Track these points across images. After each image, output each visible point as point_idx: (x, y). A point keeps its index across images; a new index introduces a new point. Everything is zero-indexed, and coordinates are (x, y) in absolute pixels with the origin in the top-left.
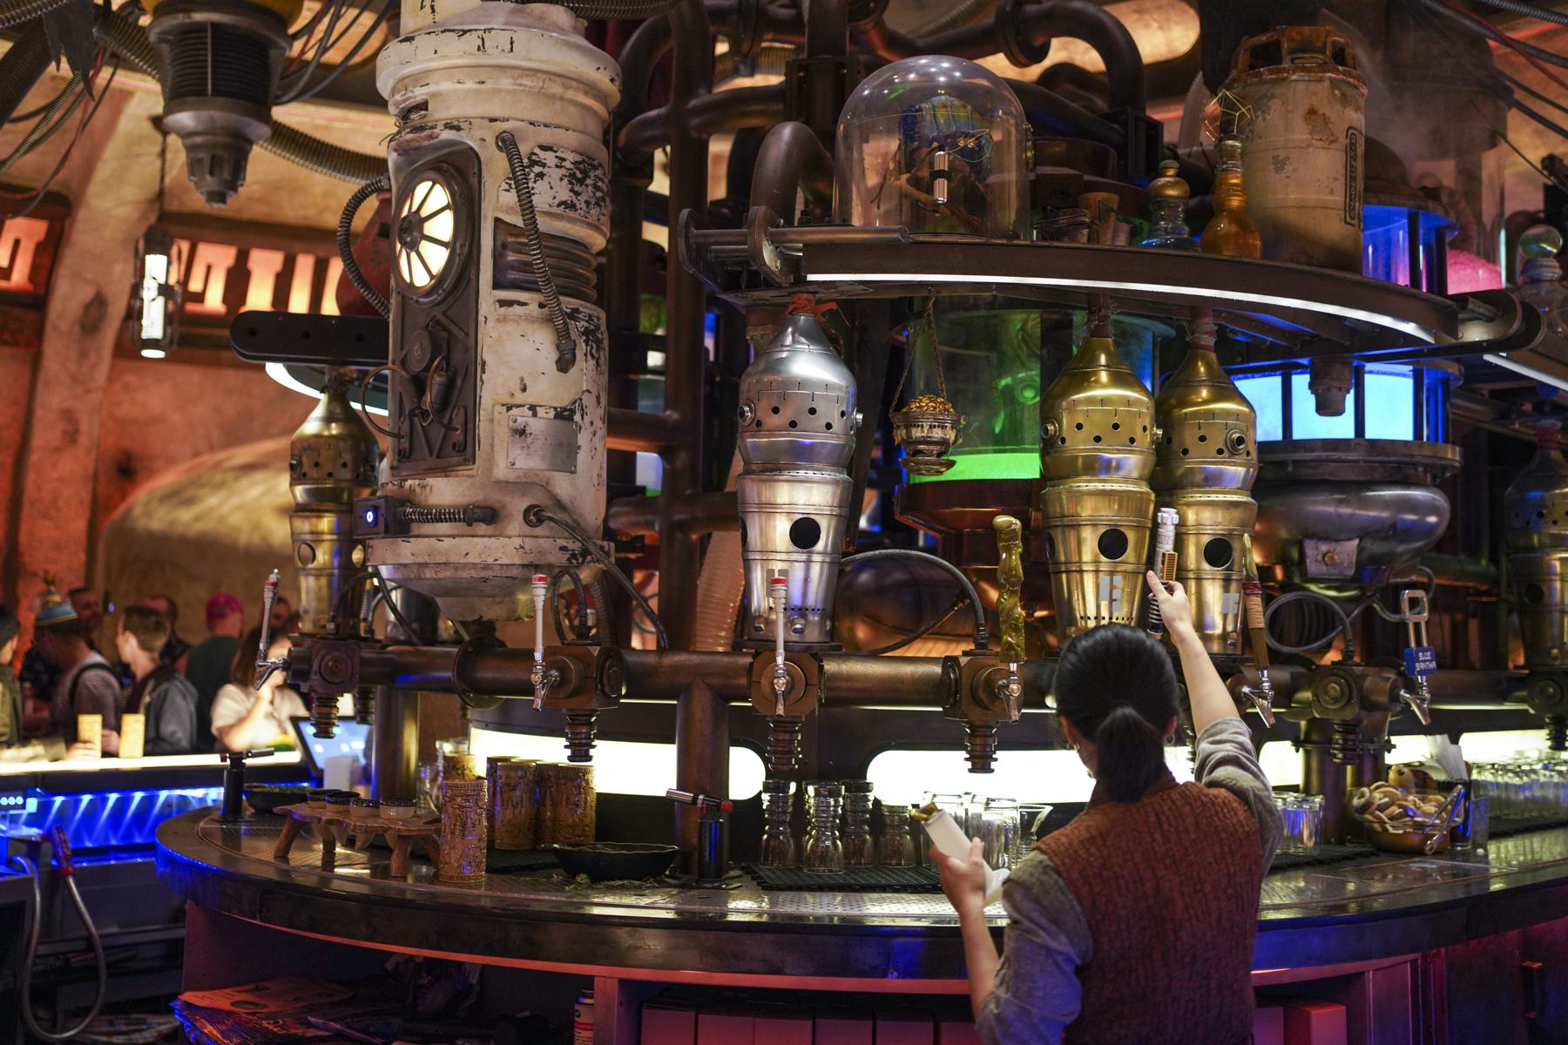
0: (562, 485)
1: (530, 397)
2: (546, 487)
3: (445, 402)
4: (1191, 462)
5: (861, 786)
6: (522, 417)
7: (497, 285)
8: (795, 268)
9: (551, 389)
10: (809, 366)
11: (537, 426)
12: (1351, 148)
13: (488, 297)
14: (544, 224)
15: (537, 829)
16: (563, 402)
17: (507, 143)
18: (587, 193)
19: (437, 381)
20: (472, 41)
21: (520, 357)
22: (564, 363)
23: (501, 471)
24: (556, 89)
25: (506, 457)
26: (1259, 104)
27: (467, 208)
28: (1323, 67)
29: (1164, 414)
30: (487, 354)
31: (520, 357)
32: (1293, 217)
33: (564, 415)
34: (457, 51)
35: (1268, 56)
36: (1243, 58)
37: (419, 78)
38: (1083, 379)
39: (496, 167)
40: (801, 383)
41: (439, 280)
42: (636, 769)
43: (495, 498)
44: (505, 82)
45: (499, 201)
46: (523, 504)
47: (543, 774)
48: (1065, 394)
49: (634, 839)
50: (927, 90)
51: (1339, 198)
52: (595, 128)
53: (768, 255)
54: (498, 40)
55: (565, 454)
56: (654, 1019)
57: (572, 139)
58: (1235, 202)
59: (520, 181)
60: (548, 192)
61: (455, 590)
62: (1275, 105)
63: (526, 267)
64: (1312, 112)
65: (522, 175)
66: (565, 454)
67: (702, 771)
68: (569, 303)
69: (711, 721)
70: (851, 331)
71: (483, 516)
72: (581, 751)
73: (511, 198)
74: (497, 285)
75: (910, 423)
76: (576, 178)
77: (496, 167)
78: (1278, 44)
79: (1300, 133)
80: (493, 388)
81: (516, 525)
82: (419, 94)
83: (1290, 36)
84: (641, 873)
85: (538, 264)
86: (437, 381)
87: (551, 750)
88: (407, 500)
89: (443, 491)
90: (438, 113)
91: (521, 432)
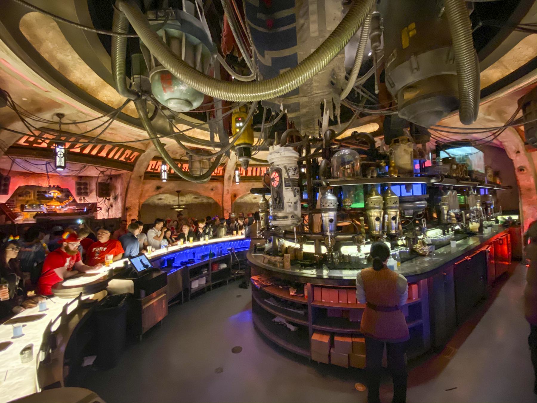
0: (296, 212)
1: (291, 201)
2: (294, 213)
3: (279, 202)
4: (389, 205)
5: (340, 252)
6: (290, 204)
7: (285, 186)
8: (328, 185)
9: (293, 200)
10: (331, 197)
11: (292, 205)
12: (411, 155)
13: (284, 188)
14: (291, 177)
15: (295, 256)
16: (295, 201)
17: (285, 167)
18: (296, 172)
19: (278, 199)
20: (279, 154)
21: (289, 196)
22: (295, 196)
23: (288, 211)
24: (291, 159)
25: (288, 209)
26: (396, 149)
27: (280, 176)
28: (406, 143)
29: (384, 199)
30: (285, 196)
31: (289, 196)
32: (403, 166)
33: (295, 203)
34: (278, 155)
35: (397, 141)
36: (393, 142)
37: (272, 159)
38: (372, 195)
39: (284, 171)
40: (330, 200)
41: (277, 186)
42: (309, 248)
43: (287, 215)
44: (284, 159)
45: (285, 175)
46: (291, 215)
47: (296, 250)
48: (368, 197)
49: (309, 261)
50: (345, 154)
51: (410, 162)
52: (296, 163)
53: (324, 183)
54: (283, 153)
55: (296, 208)
56: (315, 288)
57: (294, 165)
58: (393, 165)
59: (287, 172)
60: (291, 173)
61: (283, 227)
62: (399, 149)
63: (289, 183)
64: (405, 150)
65: (287, 171)
66: (296, 208)
67: (318, 249)
68: (295, 187)
69: (319, 242)
70: (337, 192)
71: (285, 217)
72: (301, 246)
73: (286, 175)
74: (285, 186)
75: (345, 203)
76: (294, 171)
77: (284, 171)
78: (398, 140)
79: (403, 153)
80: (286, 201)
81: (290, 218)
82: (273, 161)
83: (400, 138)
84: (310, 266)
85: (291, 183)
86: (278, 199)
87: (298, 246)
88: (276, 216)
89: (280, 214)
90: (276, 164)
91: (290, 206)
